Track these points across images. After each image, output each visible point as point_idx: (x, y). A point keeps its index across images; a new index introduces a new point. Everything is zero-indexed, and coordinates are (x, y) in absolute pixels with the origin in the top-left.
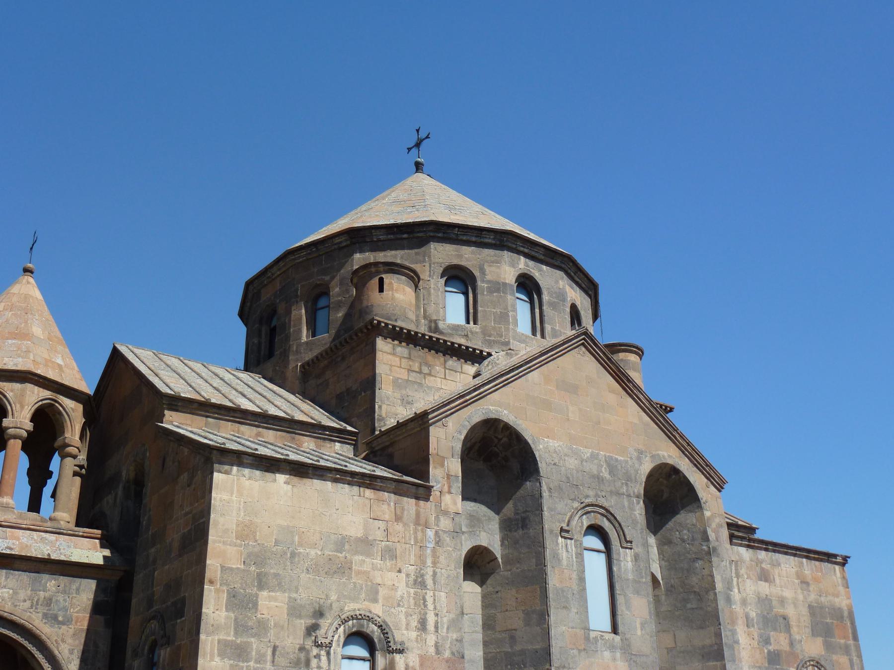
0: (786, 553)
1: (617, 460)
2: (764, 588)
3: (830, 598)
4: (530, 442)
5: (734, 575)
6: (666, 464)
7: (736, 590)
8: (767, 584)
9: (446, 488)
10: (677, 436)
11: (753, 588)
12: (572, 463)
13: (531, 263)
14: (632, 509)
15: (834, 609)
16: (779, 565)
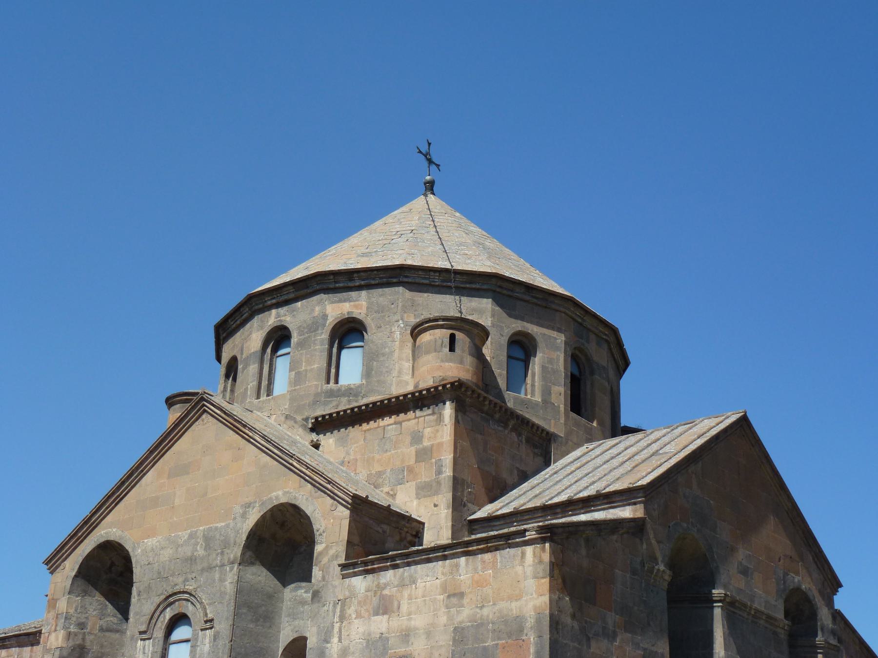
0: (429, 561)
1: (216, 528)
2: (380, 624)
3: (502, 605)
4: (130, 550)
5: (336, 619)
6: (282, 504)
7: (335, 640)
8: (386, 617)
9: (53, 627)
10: (295, 464)
11: (361, 630)
12: (166, 554)
13: (282, 310)
14: (222, 580)
15: (506, 622)
16: (414, 581)
